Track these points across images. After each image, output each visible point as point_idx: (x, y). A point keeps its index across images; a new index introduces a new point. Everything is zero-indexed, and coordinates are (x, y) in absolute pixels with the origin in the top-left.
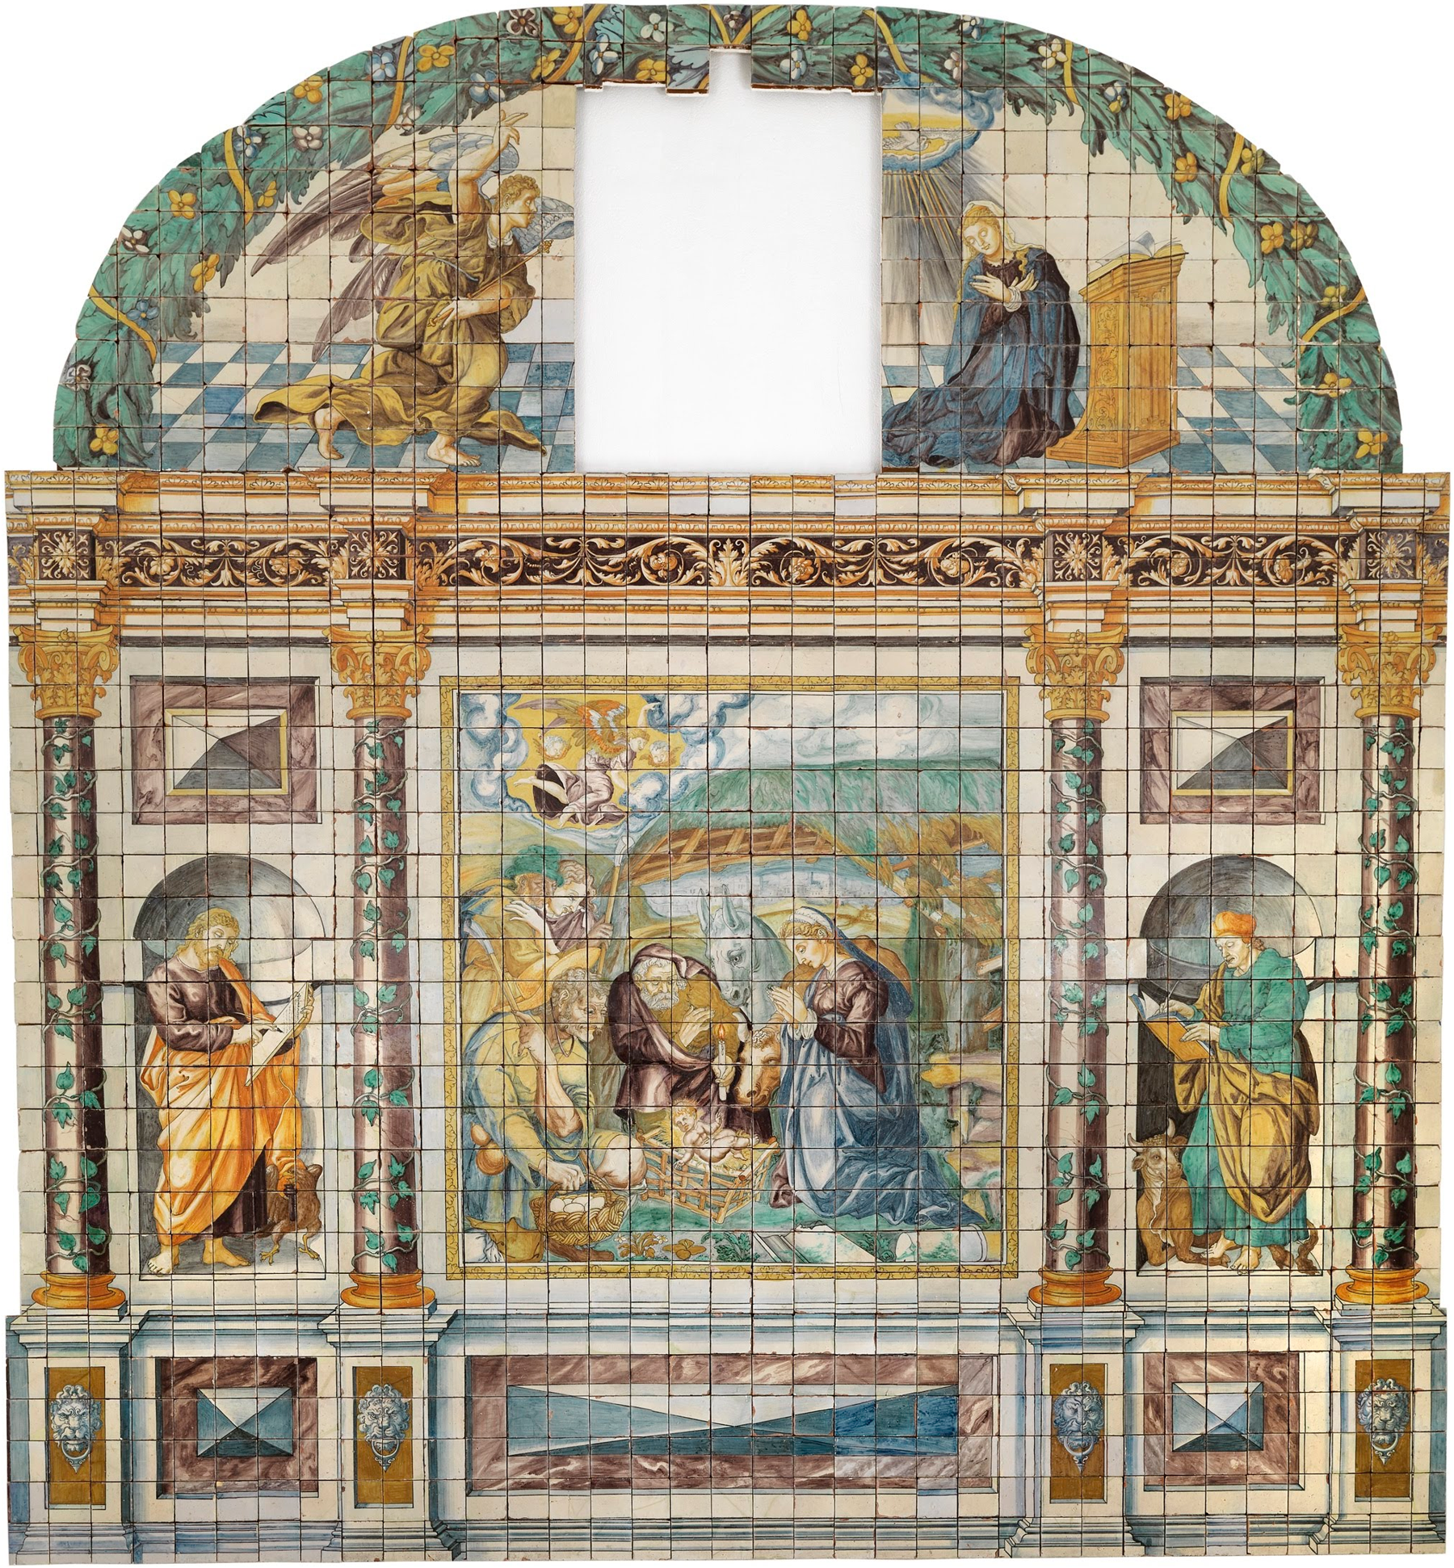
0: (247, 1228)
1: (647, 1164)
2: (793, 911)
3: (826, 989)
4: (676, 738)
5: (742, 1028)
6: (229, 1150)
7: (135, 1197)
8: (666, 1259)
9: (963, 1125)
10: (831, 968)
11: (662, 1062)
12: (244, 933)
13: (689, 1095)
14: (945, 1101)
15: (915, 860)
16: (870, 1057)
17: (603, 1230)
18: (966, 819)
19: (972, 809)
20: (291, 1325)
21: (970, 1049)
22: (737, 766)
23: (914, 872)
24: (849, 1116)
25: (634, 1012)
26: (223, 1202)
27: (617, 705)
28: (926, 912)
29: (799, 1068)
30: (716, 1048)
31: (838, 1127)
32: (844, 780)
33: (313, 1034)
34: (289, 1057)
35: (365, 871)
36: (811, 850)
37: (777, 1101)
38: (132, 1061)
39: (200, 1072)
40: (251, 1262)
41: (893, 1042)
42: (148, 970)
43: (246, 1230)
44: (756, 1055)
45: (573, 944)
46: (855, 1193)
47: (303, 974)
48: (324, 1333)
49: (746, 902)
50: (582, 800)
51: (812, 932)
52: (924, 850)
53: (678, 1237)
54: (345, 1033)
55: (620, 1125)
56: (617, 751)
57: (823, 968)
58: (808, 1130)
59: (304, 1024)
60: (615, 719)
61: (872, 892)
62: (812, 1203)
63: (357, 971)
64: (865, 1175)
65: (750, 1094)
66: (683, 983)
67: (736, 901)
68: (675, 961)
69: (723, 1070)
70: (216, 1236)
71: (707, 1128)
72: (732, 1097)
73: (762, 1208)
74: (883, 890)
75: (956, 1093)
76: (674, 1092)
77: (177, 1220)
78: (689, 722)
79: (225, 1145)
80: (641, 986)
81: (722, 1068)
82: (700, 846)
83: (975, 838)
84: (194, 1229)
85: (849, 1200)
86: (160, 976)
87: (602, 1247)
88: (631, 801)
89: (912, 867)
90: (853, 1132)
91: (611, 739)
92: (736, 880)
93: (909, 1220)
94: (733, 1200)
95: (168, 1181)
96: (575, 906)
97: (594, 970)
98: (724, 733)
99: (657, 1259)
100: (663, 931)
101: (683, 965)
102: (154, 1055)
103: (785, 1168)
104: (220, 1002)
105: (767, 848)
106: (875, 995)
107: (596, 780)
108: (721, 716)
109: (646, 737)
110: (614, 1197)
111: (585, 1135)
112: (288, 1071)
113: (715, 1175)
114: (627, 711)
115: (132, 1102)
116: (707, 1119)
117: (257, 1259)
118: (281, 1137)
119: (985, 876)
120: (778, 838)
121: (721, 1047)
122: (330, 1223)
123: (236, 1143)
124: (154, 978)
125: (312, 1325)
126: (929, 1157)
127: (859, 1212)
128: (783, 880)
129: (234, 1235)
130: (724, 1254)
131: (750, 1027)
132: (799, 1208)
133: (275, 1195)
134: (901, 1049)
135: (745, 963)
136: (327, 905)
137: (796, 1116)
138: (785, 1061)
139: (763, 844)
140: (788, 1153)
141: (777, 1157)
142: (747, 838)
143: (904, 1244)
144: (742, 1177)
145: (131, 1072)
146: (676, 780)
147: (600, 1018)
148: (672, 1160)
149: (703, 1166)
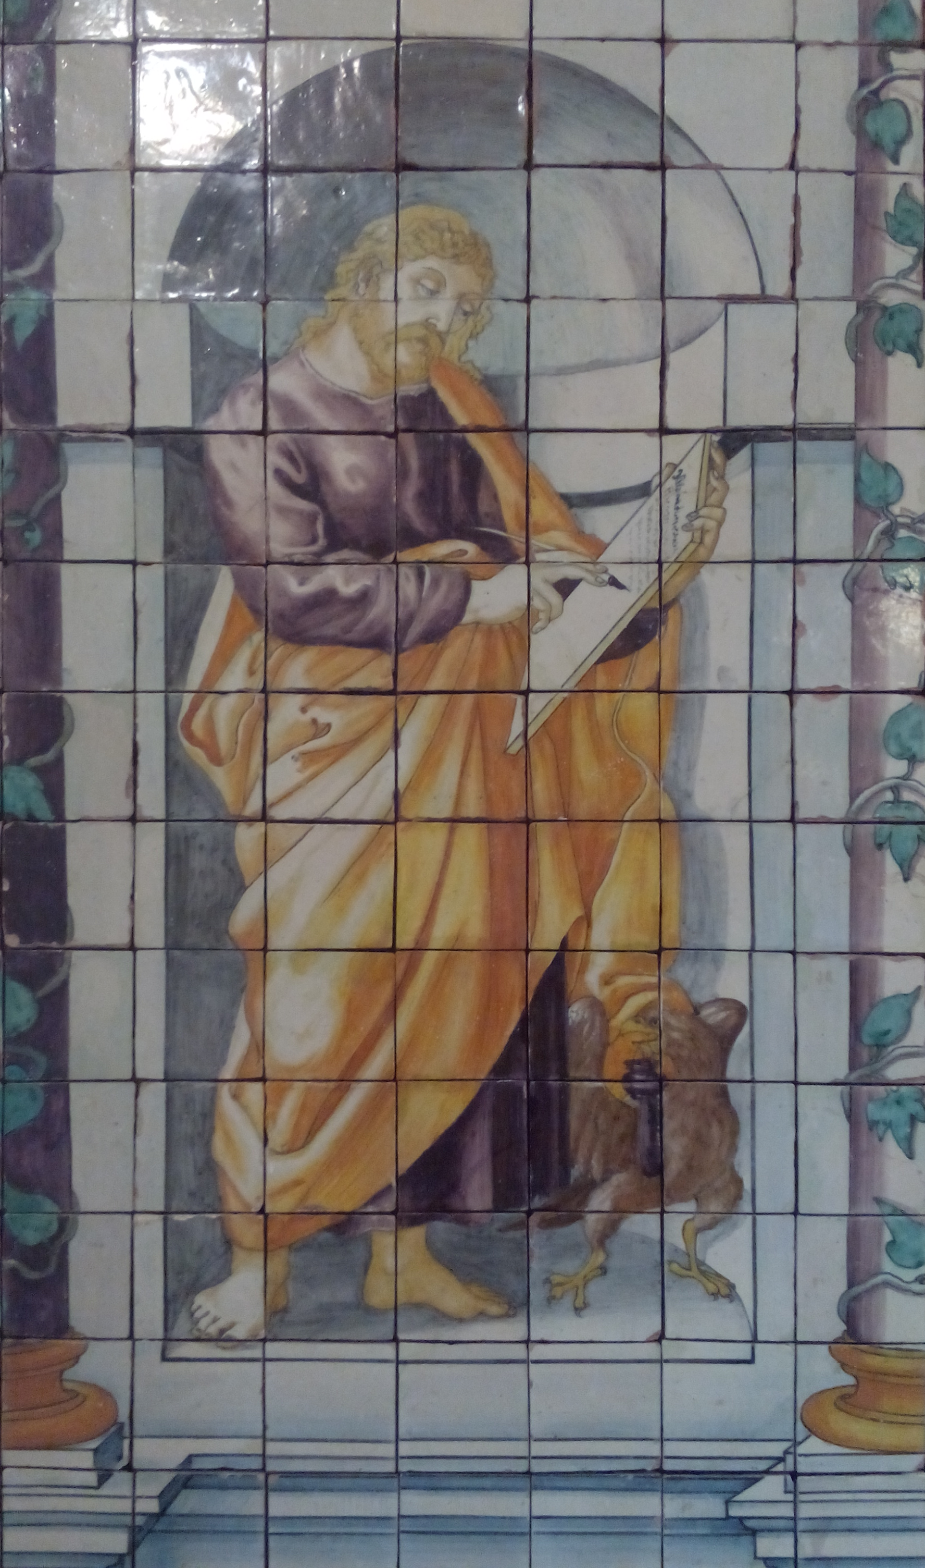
0: (506, 1196)
6: (454, 950)
7: (154, 1098)
12: (510, 280)
20: (645, 1505)
26: (429, 1115)
33: (722, 594)
34: (644, 666)
35: (891, 93)
38: (153, 674)
39: (368, 706)
40: (518, 1305)
42: (208, 391)
43: (502, 1202)
47: (694, 406)
48: (746, 1530)
54: (825, 596)
59: (695, 563)
63: (867, 396)
70: (405, 1218)
77: (283, 1169)
79: (441, 934)
84: (341, 1196)
86: (245, 411)
95: (259, 1046)
102: (223, 658)
104: (433, 494)
112: (642, 707)
115: (152, 799)
117: (537, 1295)
118: (616, 914)
122: (773, 1190)
123: (476, 931)
124: (224, 419)
125: (708, 1506)
129: (462, 1216)
133: (593, 1094)
136: (769, 199)
145: (152, 710)
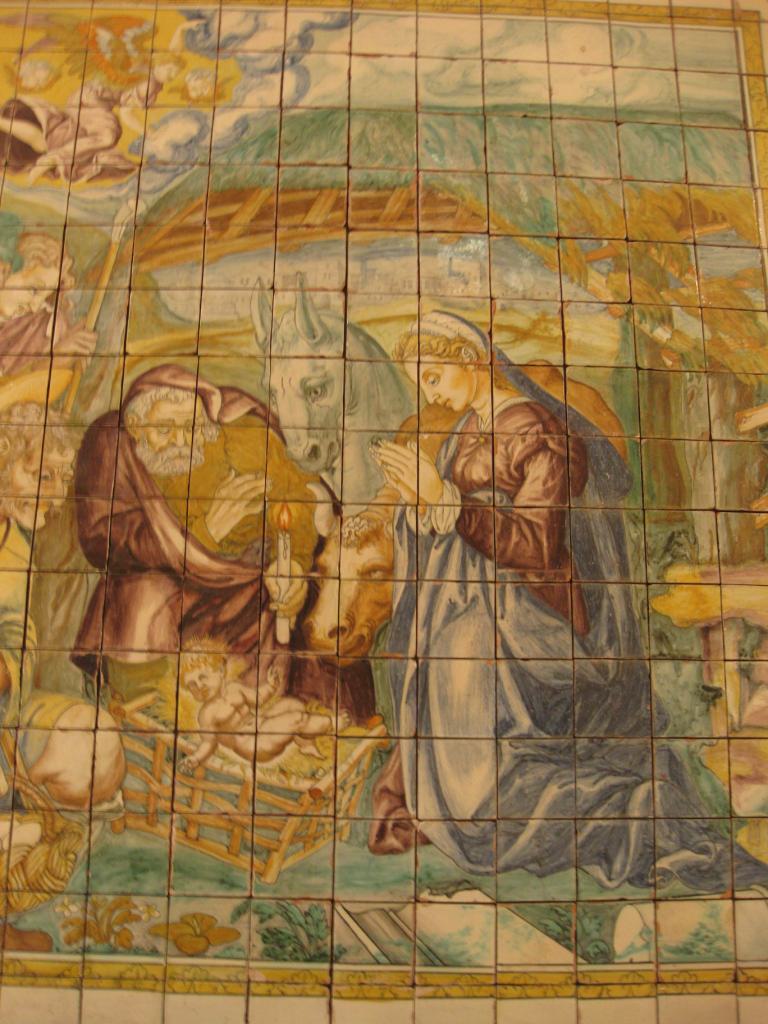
1: (126, 762)
2: (418, 317)
3: (477, 447)
4: (228, 67)
5: (322, 511)
8: (154, 952)
9: (731, 695)
10: (485, 413)
11: (166, 569)
13: (214, 631)
14: (697, 651)
15: (623, 249)
16: (559, 569)
17: (34, 887)
18: (697, 193)
19: (705, 179)
21: (734, 559)
22: (328, 102)
23: (619, 266)
24: (521, 677)
25: (121, 478)
27: (140, 22)
28: (646, 327)
29: (426, 587)
30: (273, 546)
31: (500, 698)
32: (500, 129)
36: (448, 225)
37: (385, 646)
41: (600, 544)
44: (347, 562)
45: (27, 362)
46: (533, 825)
49: (337, 301)
50: (70, 147)
51: (451, 352)
52: (635, 233)
53: (179, 909)
55: (80, 684)
56: (134, 81)
57: (470, 411)
58: (444, 701)
60: (138, 41)
61: (553, 291)
62: (451, 847)
64: (552, 792)
65: (337, 632)
66: (213, 432)
67: (318, 298)
68: (202, 395)
69: (285, 584)
71: (251, 696)
72: (301, 636)
73: (353, 854)
74: (570, 290)
75: (715, 636)
76: (184, 625)
78: (249, 45)
80: (137, 435)
81: (284, 582)
82: (262, 215)
83: (715, 220)
85: (523, 839)
87: (29, 922)
88: (149, 148)
89: (617, 257)
90: (529, 707)
91: (126, 64)
92: (321, 265)
93: (638, 879)
94: (296, 837)
96: (39, 302)
97: (59, 405)
98: (309, 60)
99: (137, 951)
100: (186, 343)
101: (216, 401)
103: (399, 775)
105: (375, 219)
106: (564, 461)
107: (97, 120)
108: (305, 39)
109: (181, 63)
110: (59, 824)
111: (13, 702)
113: (264, 787)
114: (155, 31)
116: (252, 677)
119: (737, 277)
120: (393, 207)
121: (283, 544)
126: (672, 759)
127: (542, 863)
128: (401, 268)
130: (276, 945)
131: (337, 508)
132: (425, 854)
134: (612, 555)
135: (333, 398)
137: (422, 675)
138: (402, 572)
139: (369, 213)
140: (406, 746)
141: (384, 752)
142: (340, 204)
143: (629, 927)
144: (314, 793)
146: (224, 123)
147: (60, 489)
148: (175, 756)
149: (240, 768)
